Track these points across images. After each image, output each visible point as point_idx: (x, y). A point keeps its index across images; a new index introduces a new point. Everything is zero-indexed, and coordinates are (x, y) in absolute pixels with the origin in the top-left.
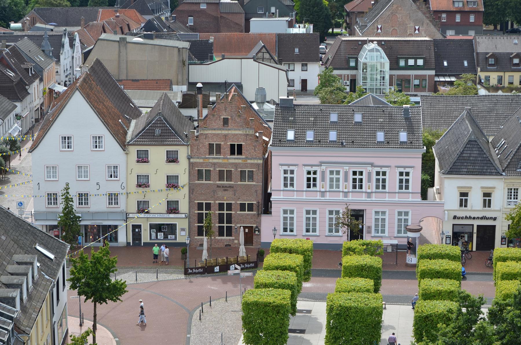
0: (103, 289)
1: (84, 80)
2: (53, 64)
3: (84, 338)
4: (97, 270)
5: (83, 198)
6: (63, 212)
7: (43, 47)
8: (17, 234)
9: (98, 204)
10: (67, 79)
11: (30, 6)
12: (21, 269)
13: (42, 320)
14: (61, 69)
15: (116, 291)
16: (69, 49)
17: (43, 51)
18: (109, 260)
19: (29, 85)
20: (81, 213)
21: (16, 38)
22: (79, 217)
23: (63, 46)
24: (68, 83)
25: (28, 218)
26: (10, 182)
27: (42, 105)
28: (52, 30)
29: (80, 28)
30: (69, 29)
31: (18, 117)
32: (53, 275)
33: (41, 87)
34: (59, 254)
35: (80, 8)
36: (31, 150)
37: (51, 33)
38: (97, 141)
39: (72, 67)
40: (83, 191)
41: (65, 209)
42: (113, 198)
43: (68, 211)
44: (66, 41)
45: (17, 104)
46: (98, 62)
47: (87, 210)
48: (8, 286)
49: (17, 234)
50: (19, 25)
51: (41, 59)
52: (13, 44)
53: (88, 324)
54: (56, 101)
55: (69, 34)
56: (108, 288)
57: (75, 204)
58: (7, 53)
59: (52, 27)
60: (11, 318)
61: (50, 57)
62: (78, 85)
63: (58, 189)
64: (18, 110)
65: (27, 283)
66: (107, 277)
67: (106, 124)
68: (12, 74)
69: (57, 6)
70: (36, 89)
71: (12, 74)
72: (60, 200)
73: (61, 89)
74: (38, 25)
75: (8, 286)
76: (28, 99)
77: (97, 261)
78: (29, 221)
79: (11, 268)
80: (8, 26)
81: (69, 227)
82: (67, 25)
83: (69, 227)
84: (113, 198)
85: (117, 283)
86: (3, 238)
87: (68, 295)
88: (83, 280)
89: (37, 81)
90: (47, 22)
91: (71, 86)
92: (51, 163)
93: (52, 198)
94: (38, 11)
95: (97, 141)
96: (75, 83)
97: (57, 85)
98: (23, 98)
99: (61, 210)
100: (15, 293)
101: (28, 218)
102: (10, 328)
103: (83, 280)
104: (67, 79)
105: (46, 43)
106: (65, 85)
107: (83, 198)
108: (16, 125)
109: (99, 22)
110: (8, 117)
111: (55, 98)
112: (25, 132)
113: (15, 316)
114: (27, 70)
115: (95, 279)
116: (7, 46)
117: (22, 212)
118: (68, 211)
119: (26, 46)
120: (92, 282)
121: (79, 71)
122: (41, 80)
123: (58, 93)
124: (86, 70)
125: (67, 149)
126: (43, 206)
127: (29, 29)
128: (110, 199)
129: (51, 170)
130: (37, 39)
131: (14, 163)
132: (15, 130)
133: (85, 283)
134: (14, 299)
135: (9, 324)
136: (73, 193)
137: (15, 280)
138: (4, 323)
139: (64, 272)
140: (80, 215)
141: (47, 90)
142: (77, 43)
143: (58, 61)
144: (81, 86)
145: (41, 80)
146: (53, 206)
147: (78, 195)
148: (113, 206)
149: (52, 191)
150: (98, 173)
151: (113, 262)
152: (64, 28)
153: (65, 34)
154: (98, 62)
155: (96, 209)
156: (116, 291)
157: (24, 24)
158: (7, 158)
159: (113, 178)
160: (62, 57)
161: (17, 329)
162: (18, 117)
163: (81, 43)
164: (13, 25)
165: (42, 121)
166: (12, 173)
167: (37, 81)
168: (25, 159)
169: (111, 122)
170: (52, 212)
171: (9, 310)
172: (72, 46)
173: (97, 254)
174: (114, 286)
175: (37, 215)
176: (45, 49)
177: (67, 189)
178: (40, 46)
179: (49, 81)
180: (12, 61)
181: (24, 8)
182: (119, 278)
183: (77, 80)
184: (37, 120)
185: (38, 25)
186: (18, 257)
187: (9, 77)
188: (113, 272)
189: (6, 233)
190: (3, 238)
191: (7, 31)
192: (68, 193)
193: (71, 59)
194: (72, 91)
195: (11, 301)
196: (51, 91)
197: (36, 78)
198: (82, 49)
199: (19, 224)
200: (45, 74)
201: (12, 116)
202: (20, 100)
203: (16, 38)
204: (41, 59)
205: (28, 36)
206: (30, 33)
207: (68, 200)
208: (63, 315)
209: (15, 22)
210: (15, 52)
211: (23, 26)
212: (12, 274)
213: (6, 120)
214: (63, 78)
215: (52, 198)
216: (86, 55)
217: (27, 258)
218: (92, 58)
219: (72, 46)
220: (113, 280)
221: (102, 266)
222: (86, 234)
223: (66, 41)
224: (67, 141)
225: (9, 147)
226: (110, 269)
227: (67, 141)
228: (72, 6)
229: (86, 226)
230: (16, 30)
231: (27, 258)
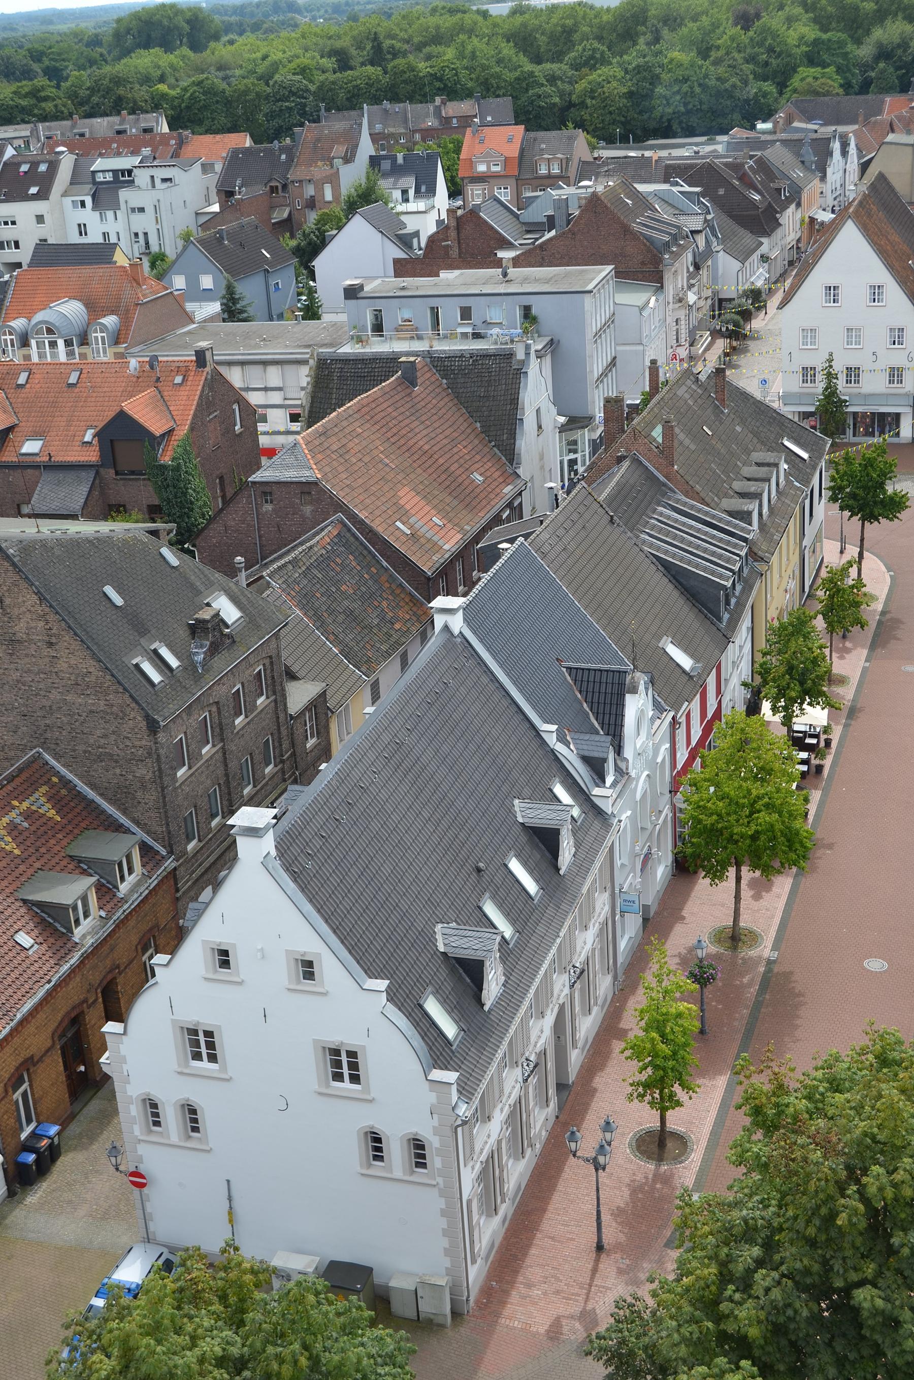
0: (875, 502)
1: (861, 203)
2: (817, 181)
3: (845, 570)
4: (868, 475)
5: (853, 373)
6: (823, 394)
7: (802, 156)
8: (758, 424)
9: (874, 383)
10: (836, 203)
11: (786, 96)
12: (762, 472)
13: (788, 543)
14: (827, 188)
15: (893, 506)
16: (840, 158)
17: (803, 162)
18: (886, 463)
19: (781, 213)
20: (850, 395)
21: (764, 145)
22: (846, 401)
23: (831, 154)
24: (837, 209)
25: (774, 401)
26: (748, 351)
27: (798, 241)
28: (816, 131)
29: (856, 127)
30: (841, 129)
31: (764, 258)
32: (806, 481)
33: (799, 215)
34: (816, 455)
35: (858, 97)
36: (782, 305)
37: (815, 136)
38: (876, 292)
39: (843, 185)
40: (853, 364)
41: (826, 389)
42: (895, 374)
43: (830, 393)
44: (836, 146)
45: (762, 240)
46: (881, 177)
47: (858, 390)
48: (743, 495)
49: (758, 424)
50: (768, 126)
51: (798, 173)
52: (759, 153)
53: (852, 551)
54: (819, 234)
55: (841, 137)
56: (882, 501)
57: (841, 383)
58: (751, 167)
59: (815, 127)
60: (745, 540)
61: (813, 171)
62: (851, 210)
63: (818, 361)
64: (764, 249)
65: (769, 492)
66: (881, 486)
67: (890, 267)
68: (757, 197)
69: (824, 95)
70: (791, 221)
71: (757, 197)
72: (820, 377)
73: (826, 217)
74: (796, 124)
75: (743, 495)
76: (779, 232)
77: (869, 463)
78: (775, 405)
79: (747, 471)
80: (753, 127)
81: (831, 416)
82: (839, 122)
83: (831, 416)
84: (895, 374)
85: (895, 494)
86: (738, 429)
87: (824, 510)
88: (848, 490)
89: (793, 206)
90: (809, 119)
91: (842, 214)
92: (808, 325)
93: (808, 373)
94: (796, 104)
95: (876, 292)
96: (846, 208)
97: (820, 211)
98: (773, 231)
99: (820, 390)
100: (753, 506)
101: (774, 401)
102: (743, 553)
103: (848, 490)
104: (836, 203)
105: (807, 150)
106: (833, 212)
107: (853, 373)
108: (761, 270)
109: (885, 116)
110: (751, 259)
111: (818, 231)
112: (773, 280)
113: (750, 537)
114: (778, 190)
115: (865, 488)
116: (751, 157)
117: (766, 393)
118: (830, 393)
119: (778, 155)
120: (860, 492)
121: (854, 190)
122: (799, 205)
123: (822, 224)
124: (864, 188)
125: (832, 304)
126: (795, 384)
127: (784, 131)
128: (891, 375)
129: (809, 334)
130: (794, 145)
131: (757, 323)
132: (759, 278)
133: (849, 493)
134: (750, 513)
135: (742, 548)
136: (838, 367)
137: (753, 487)
138: (735, 546)
139: (821, 478)
140: (847, 398)
141: (807, 220)
142: (852, 149)
143: (823, 178)
144: (856, 212)
145: (799, 205)
146: (809, 385)
147: (845, 371)
148: (895, 385)
149: (809, 364)
150: (876, 337)
151: (891, 466)
152: (833, 128)
153: (835, 137)
154: (881, 177)
155: (870, 391)
156: (893, 506)
157: (776, 124)
158: (747, 315)
159: (896, 346)
160: (829, 171)
161: (753, 555)
162: (764, 258)
163: (858, 149)
164: (760, 126)
165: (800, 263)
166: (754, 339)
167: (793, 206)
168: (772, 318)
169: (897, 264)
170: (808, 394)
171: (743, 529)
172: (844, 153)
173: (869, 454)
174: (891, 498)
175: (786, 398)
176: (806, 159)
177: (830, 361)
178: (798, 154)
179: (810, 206)
180: (757, 178)
181: (776, 100)
182: (898, 487)
183: (850, 204)
184: (791, 263)
185: (796, 124)
186: (758, 456)
187: (752, 202)
188: (890, 479)
189: (743, 422)
190: (738, 429)
191: (752, 134)
192: (831, 367)
193: (843, 174)
194: (842, 220)
195: (745, 516)
196: (812, 220)
197: (792, 202)
198: (859, 158)
199: (761, 410)
200: (805, 196)
201: (755, 257)
202: (768, 234)
203: (764, 145)
204: (798, 173)
205: (784, 142)
206: (784, 136)
207: (830, 376)
208: (818, 538)
209: (764, 121)
210: (763, 165)
211: (775, 127)
212: (749, 480)
213: (747, 264)
214: (830, 202)
215: (808, 373)
216: (864, 167)
217: (770, 457)
218: (873, 171)
219: (844, 153)
220: (890, 489)
221: (875, 470)
222: (855, 425)
223: (836, 146)
224: (832, 292)
225: (750, 302)
226: (886, 475)
227: (832, 292)
228: (847, 94)
229: (855, 414)
230: (764, 132)
231: (770, 457)
